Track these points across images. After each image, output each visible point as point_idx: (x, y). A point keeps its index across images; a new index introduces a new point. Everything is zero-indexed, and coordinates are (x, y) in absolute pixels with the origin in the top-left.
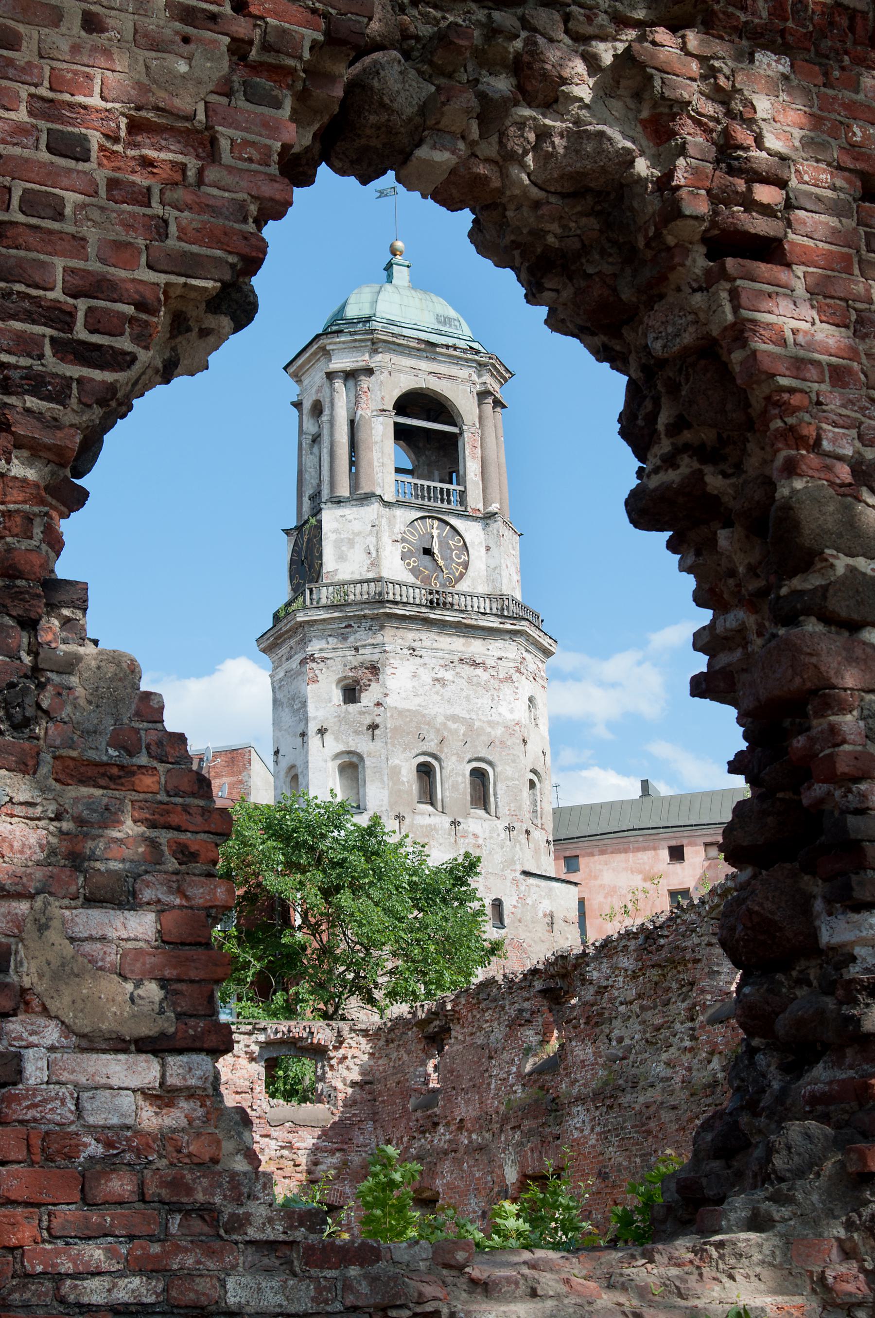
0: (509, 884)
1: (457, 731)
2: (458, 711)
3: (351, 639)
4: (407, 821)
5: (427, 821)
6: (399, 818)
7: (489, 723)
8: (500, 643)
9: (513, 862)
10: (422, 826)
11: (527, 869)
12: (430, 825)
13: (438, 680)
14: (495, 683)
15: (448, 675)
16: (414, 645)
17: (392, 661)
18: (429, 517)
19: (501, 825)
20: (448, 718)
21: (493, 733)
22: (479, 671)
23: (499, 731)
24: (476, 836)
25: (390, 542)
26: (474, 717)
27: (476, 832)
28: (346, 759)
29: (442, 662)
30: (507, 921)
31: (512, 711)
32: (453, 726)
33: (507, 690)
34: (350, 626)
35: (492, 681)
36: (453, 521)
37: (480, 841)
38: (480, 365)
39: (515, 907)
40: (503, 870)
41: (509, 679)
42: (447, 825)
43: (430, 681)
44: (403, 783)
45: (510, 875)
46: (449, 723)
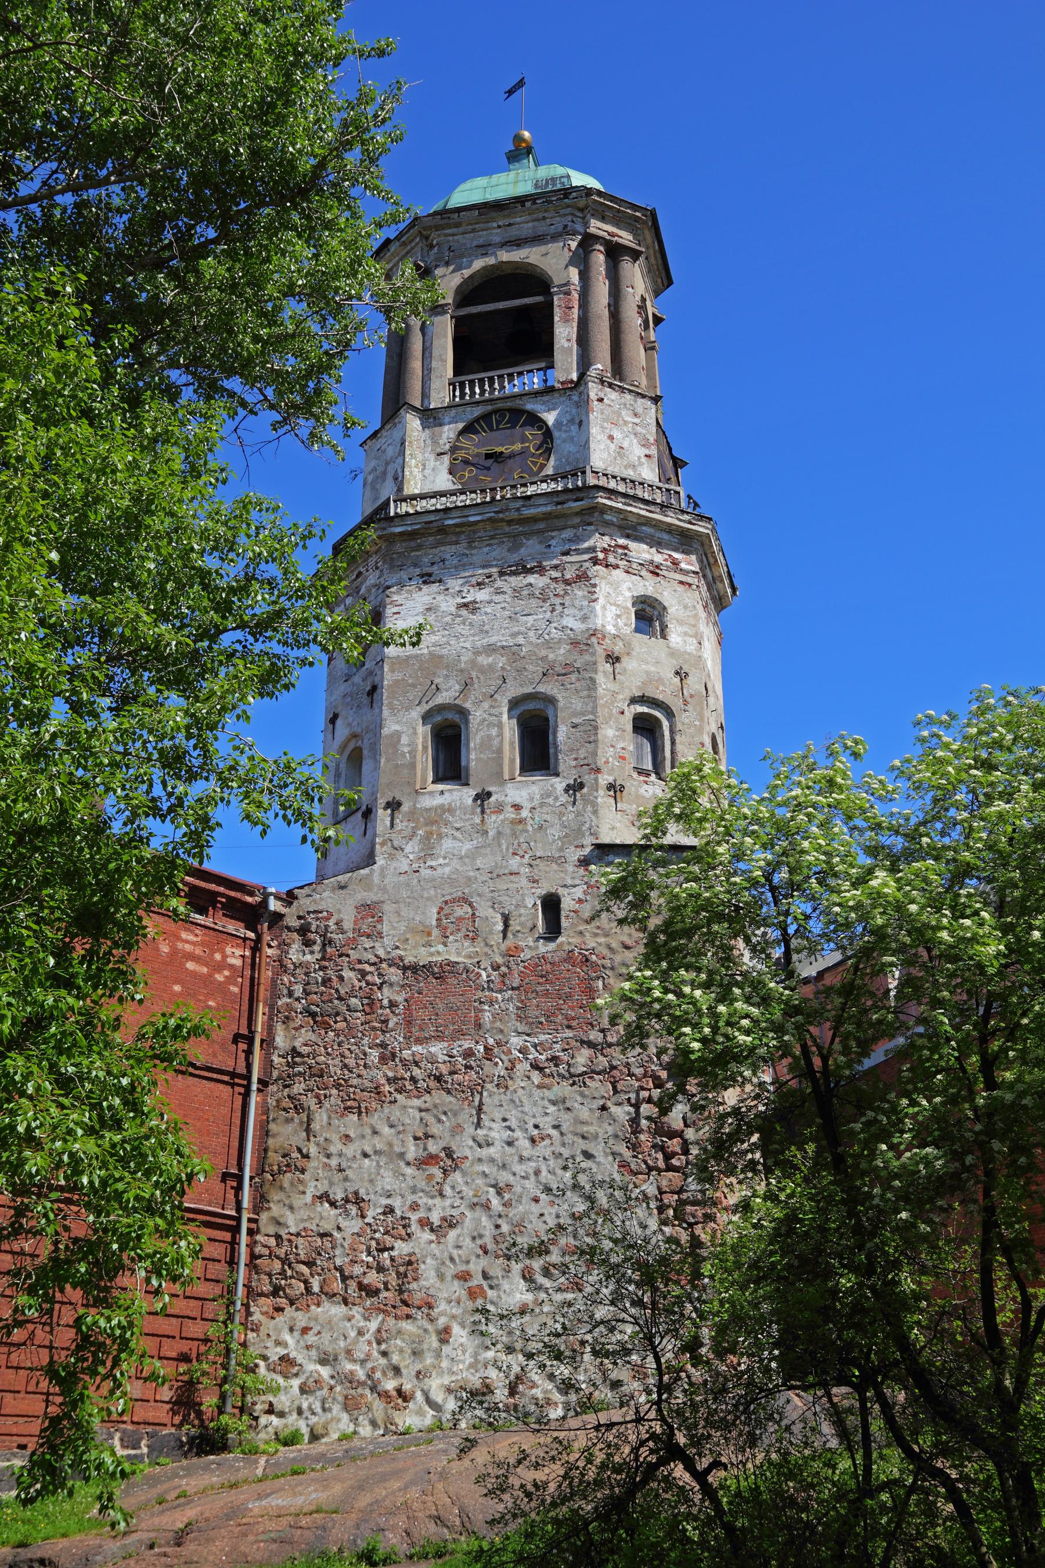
0: (571, 869)
1: (491, 667)
2: (493, 639)
3: (363, 591)
4: (405, 808)
5: (439, 801)
6: (394, 806)
7: (548, 645)
8: (567, 534)
9: (579, 832)
10: (427, 810)
11: (606, 839)
12: (442, 806)
13: (465, 605)
14: (560, 588)
15: (482, 595)
16: (429, 570)
17: (395, 597)
18: (496, 412)
19: (558, 784)
20: (477, 653)
21: (551, 656)
22: (531, 579)
23: (561, 654)
24: (517, 807)
25: (432, 457)
26: (520, 640)
27: (518, 801)
28: (351, 746)
29: (474, 581)
30: (564, 923)
31: (585, 619)
32: (484, 660)
33: (579, 592)
34: (360, 574)
35: (553, 585)
36: (529, 407)
37: (525, 813)
38: (582, 210)
39: (580, 901)
40: (561, 850)
41: (583, 577)
42: (470, 801)
43: (453, 609)
44: (403, 755)
45: (574, 855)
46: (484, 660)
